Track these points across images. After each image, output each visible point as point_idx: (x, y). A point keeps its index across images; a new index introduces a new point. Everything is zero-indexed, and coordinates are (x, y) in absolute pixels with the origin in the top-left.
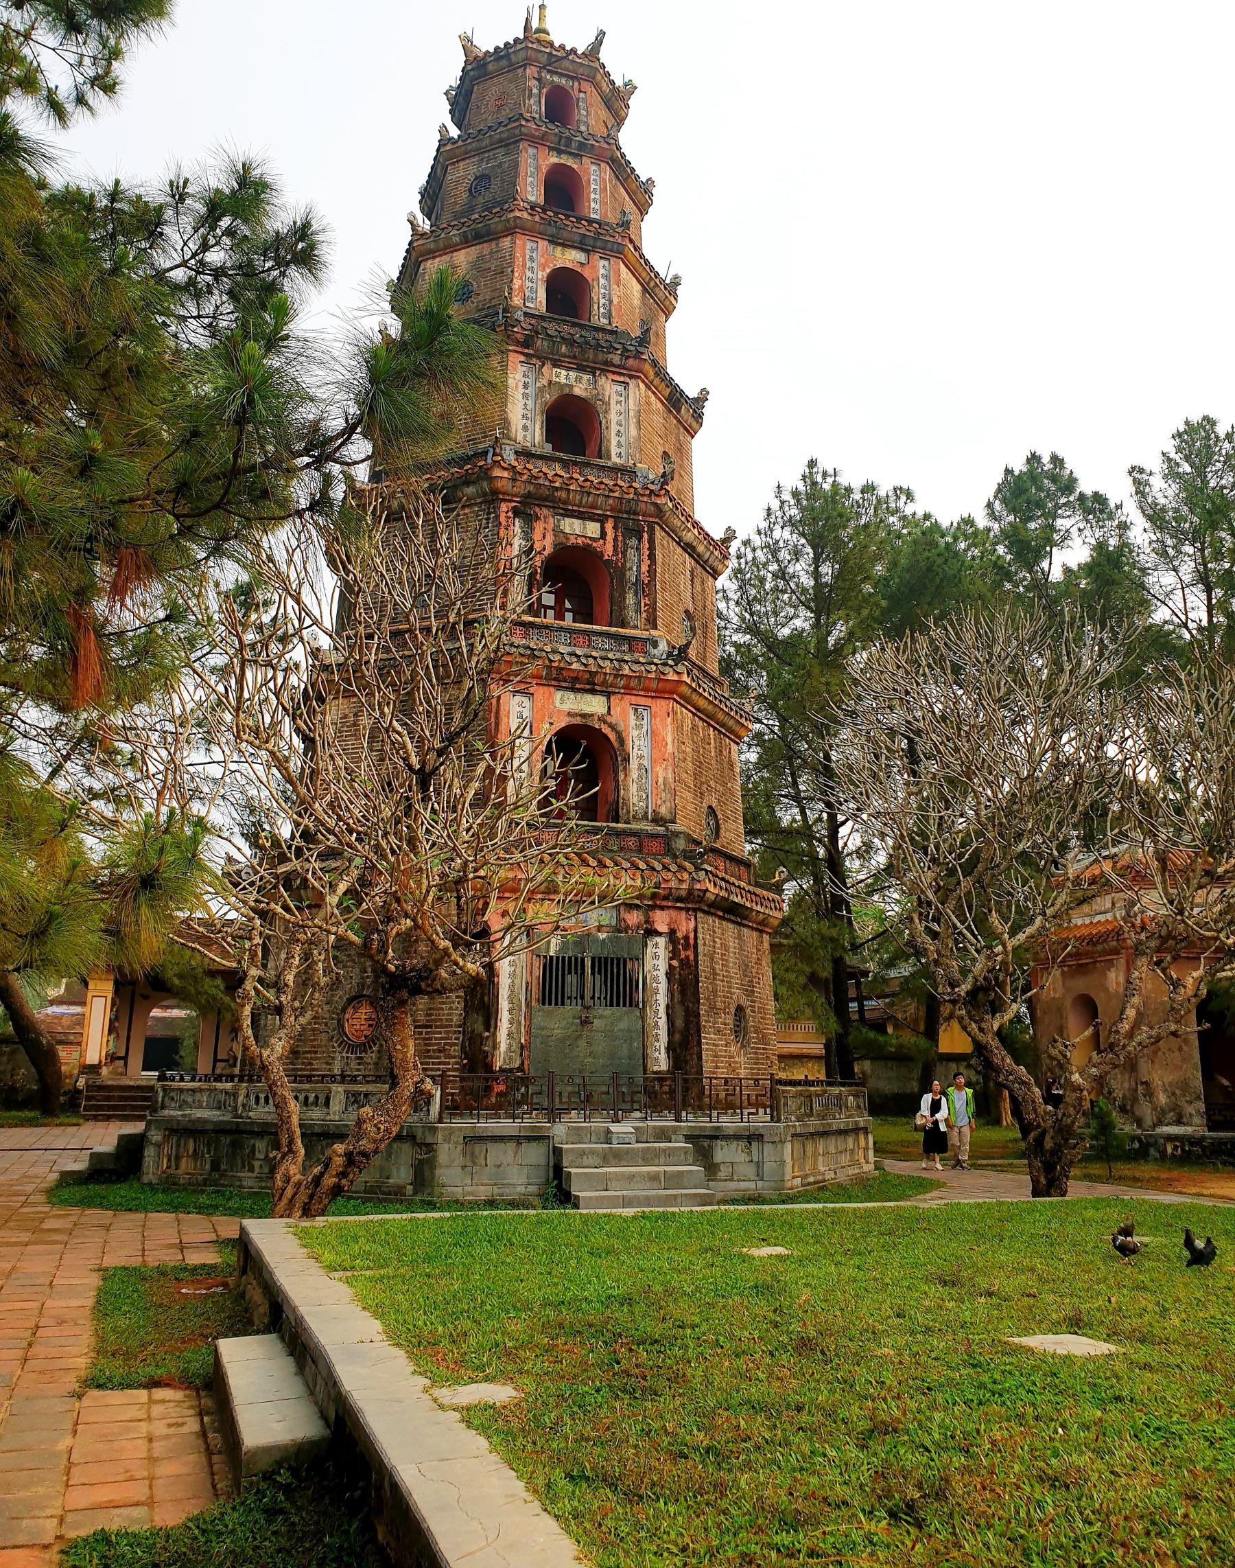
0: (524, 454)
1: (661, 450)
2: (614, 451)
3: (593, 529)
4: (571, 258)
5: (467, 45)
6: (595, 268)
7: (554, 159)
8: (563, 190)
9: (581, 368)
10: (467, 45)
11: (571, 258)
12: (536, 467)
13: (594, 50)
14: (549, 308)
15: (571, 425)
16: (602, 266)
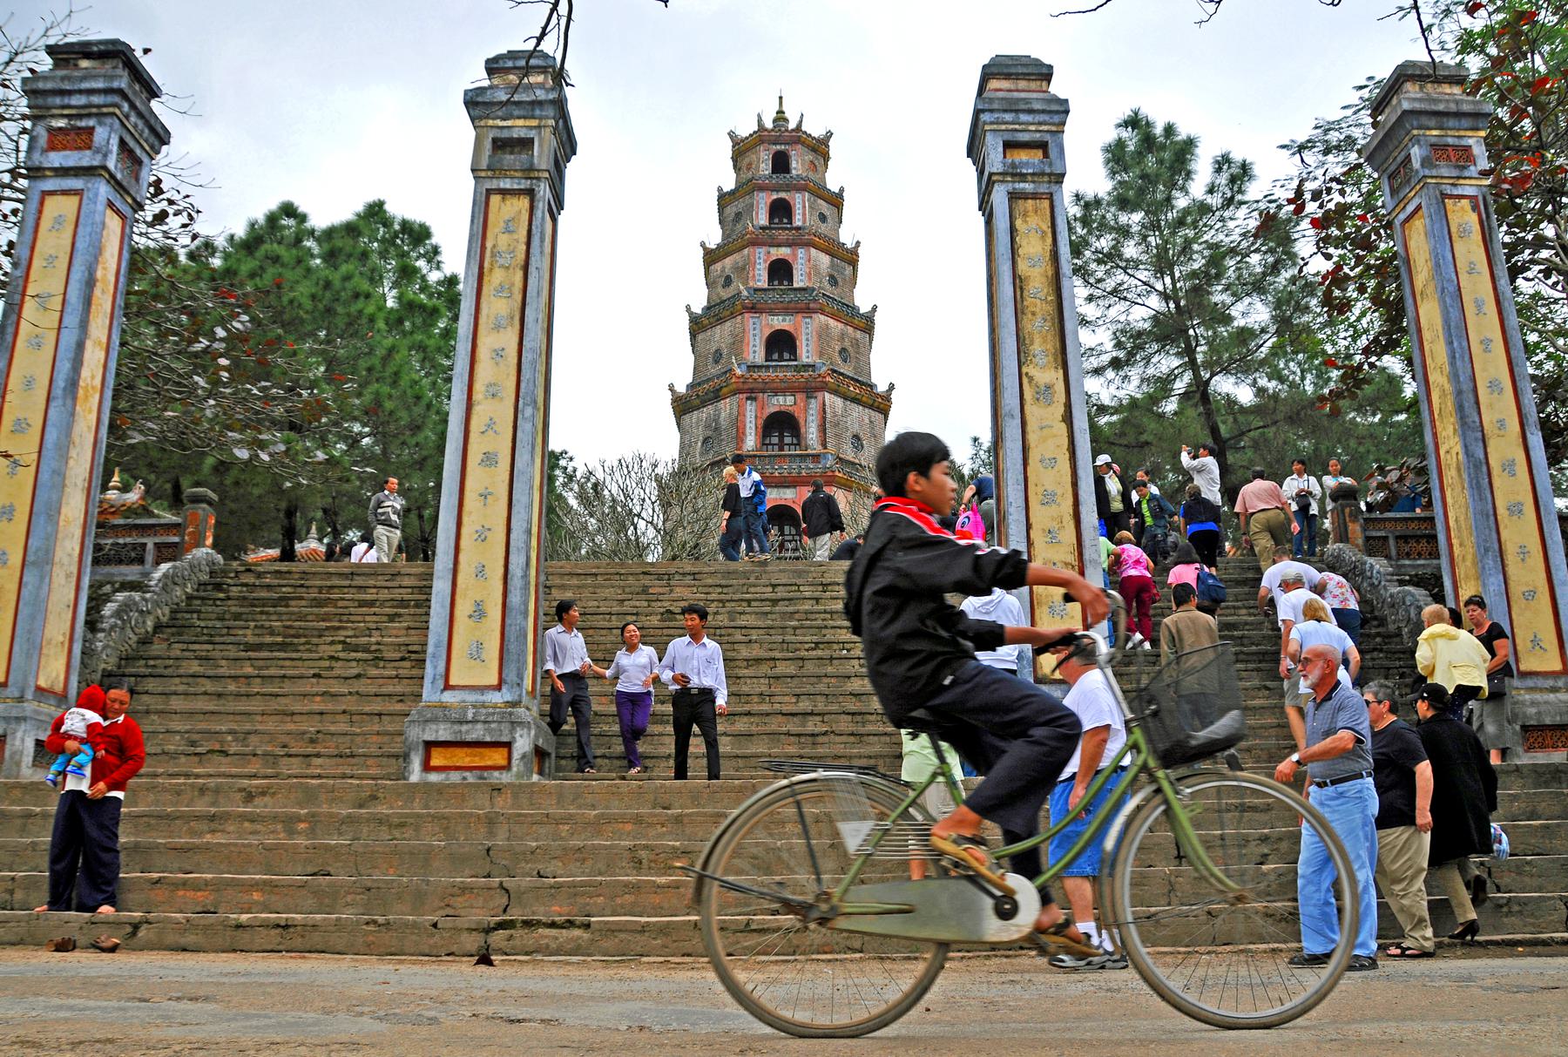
0: (752, 367)
1: (837, 348)
2: (804, 355)
3: (790, 400)
4: (783, 252)
5: (732, 135)
6: (795, 255)
7: (775, 196)
8: (781, 210)
9: (787, 314)
10: (732, 135)
11: (783, 252)
12: (763, 374)
13: (799, 128)
14: (771, 279)
15: (781, 343)
16: (801, 252)
